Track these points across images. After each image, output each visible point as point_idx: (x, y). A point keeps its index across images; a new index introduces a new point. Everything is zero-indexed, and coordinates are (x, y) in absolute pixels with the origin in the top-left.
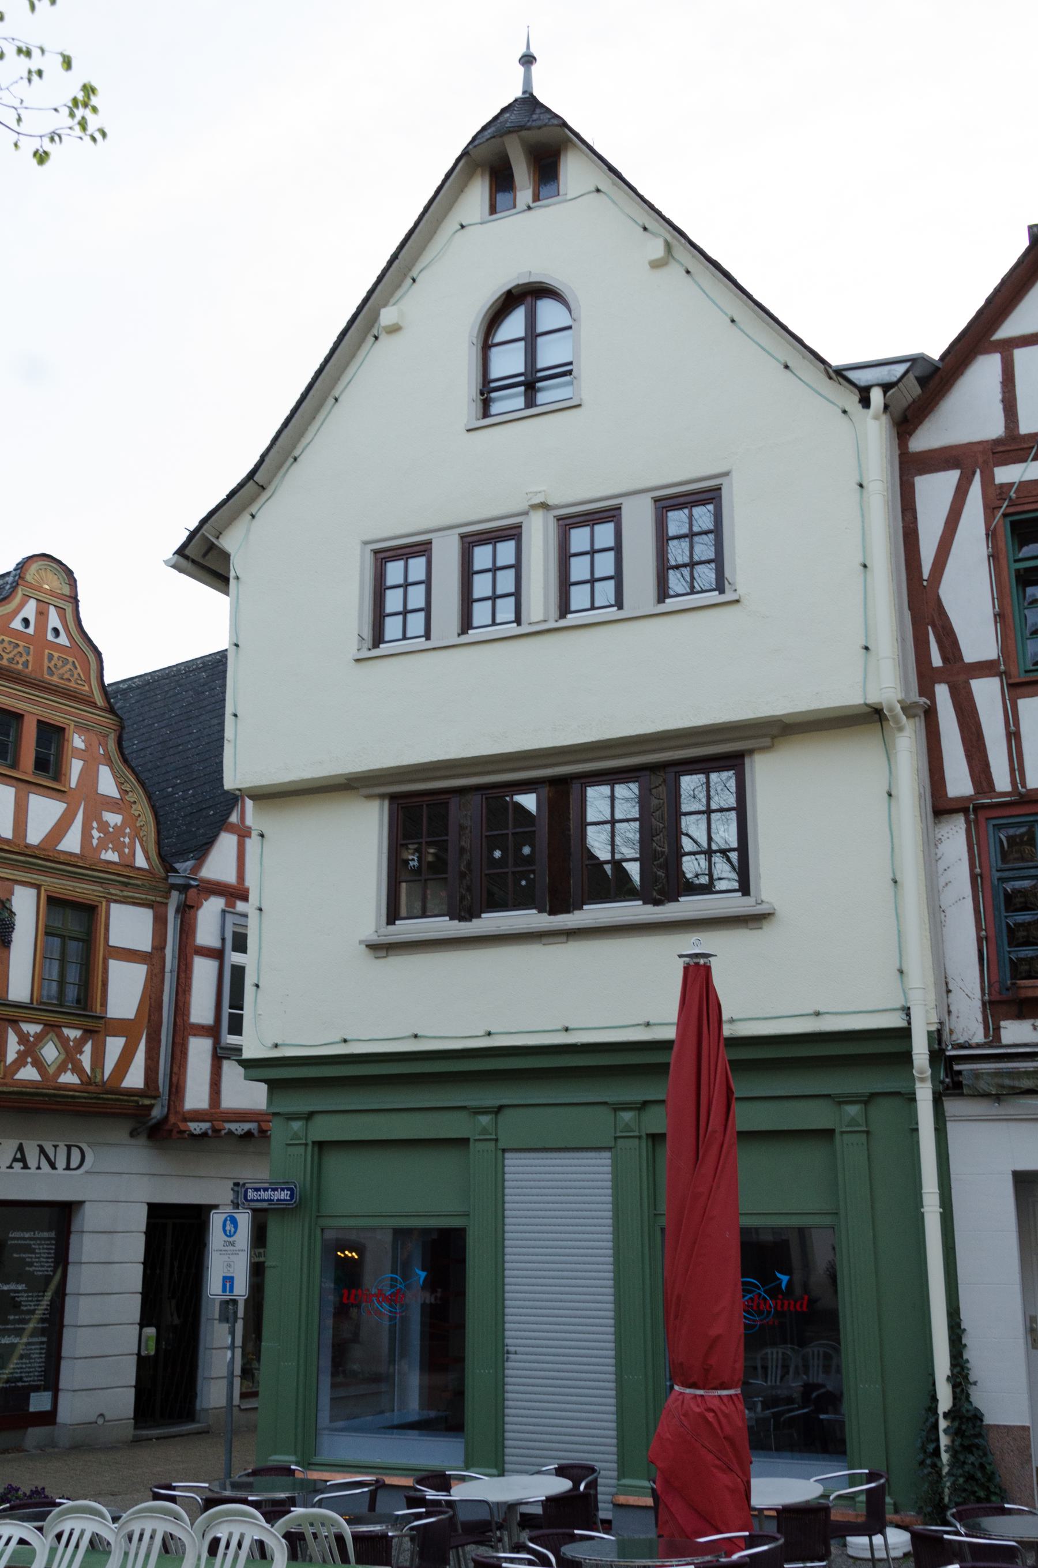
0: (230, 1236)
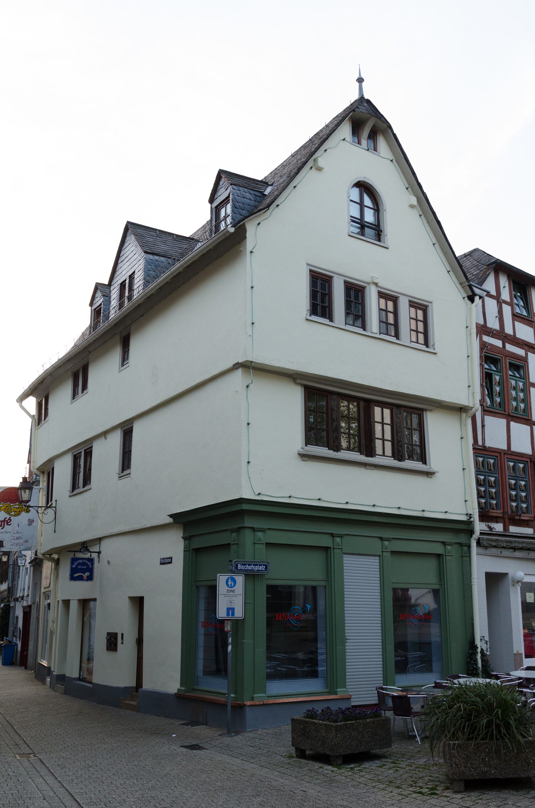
0: (231, 587)
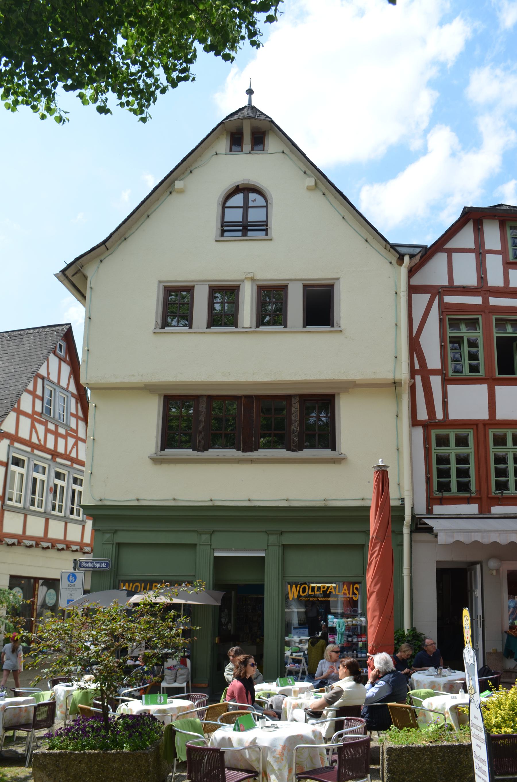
0: (72, 582)
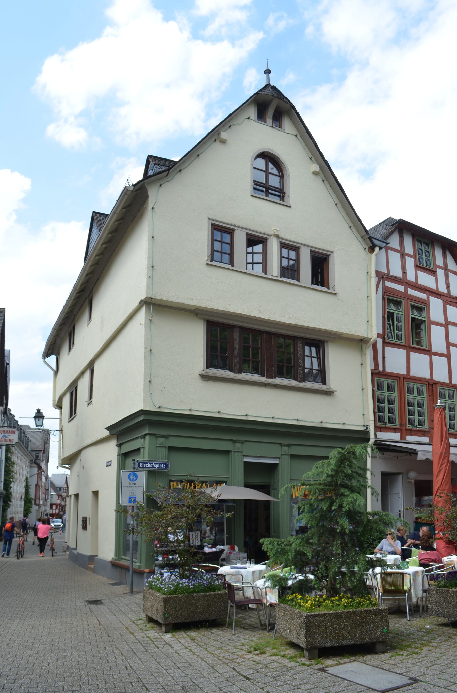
0: (133, 481)
